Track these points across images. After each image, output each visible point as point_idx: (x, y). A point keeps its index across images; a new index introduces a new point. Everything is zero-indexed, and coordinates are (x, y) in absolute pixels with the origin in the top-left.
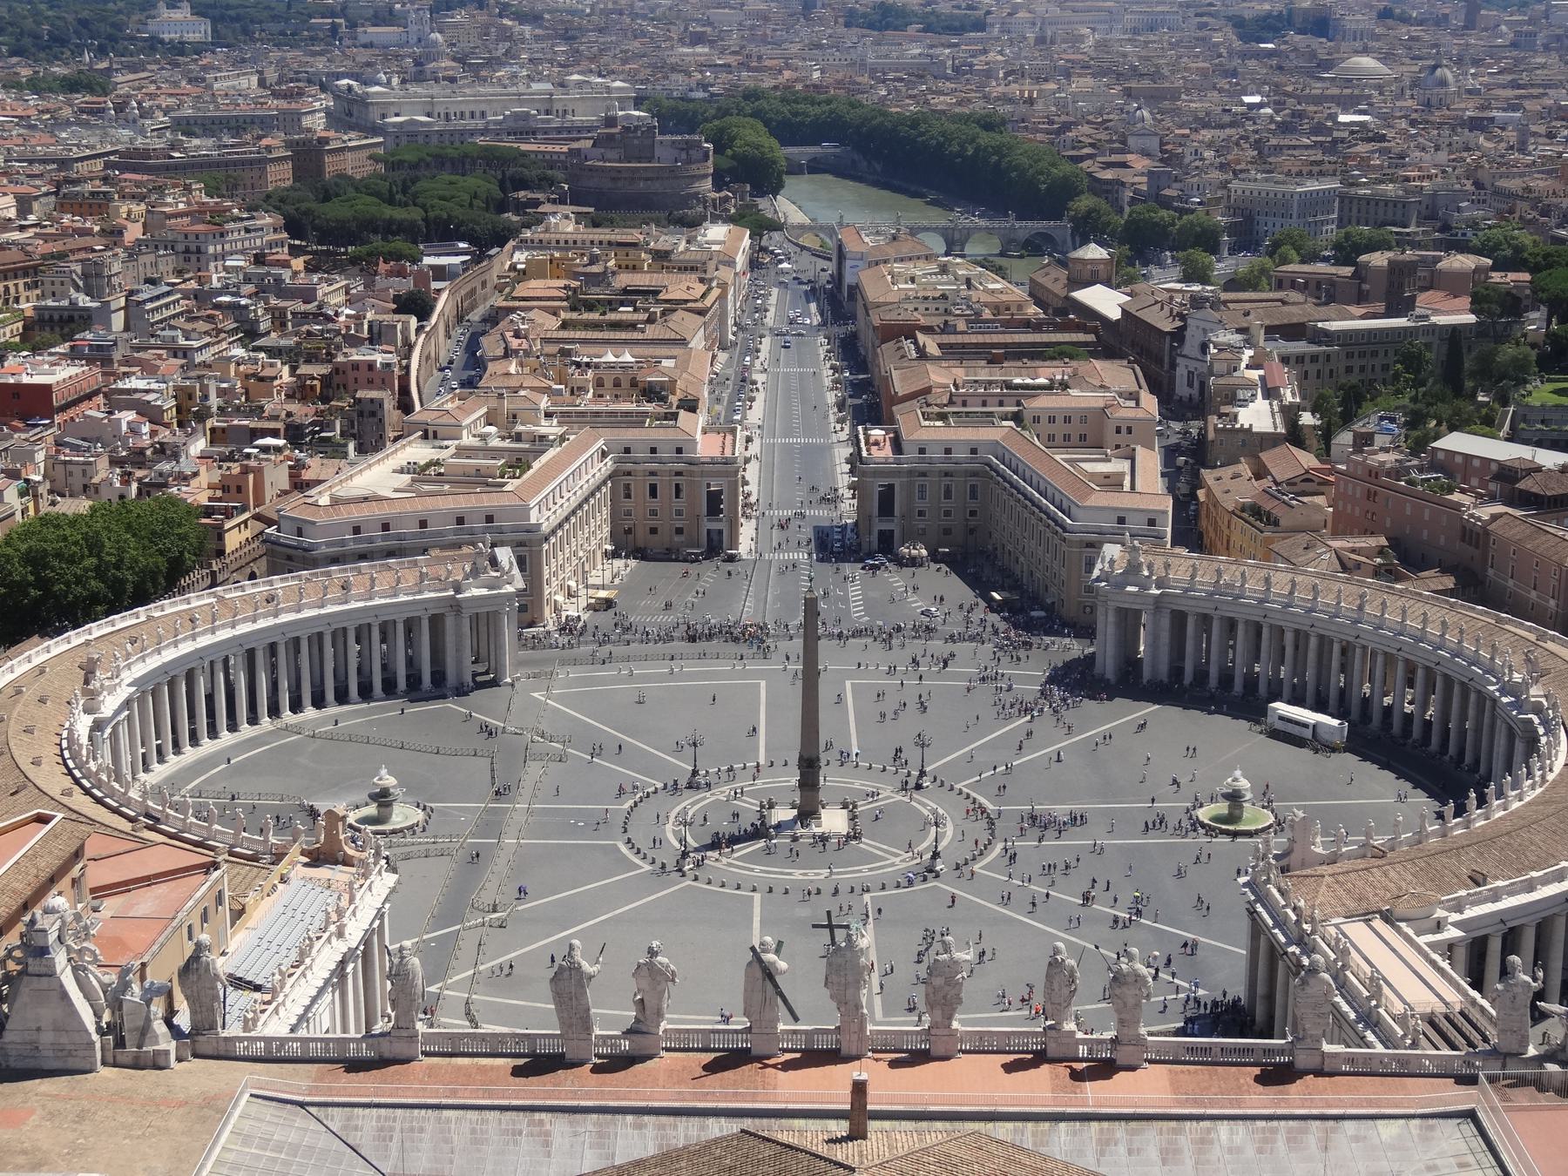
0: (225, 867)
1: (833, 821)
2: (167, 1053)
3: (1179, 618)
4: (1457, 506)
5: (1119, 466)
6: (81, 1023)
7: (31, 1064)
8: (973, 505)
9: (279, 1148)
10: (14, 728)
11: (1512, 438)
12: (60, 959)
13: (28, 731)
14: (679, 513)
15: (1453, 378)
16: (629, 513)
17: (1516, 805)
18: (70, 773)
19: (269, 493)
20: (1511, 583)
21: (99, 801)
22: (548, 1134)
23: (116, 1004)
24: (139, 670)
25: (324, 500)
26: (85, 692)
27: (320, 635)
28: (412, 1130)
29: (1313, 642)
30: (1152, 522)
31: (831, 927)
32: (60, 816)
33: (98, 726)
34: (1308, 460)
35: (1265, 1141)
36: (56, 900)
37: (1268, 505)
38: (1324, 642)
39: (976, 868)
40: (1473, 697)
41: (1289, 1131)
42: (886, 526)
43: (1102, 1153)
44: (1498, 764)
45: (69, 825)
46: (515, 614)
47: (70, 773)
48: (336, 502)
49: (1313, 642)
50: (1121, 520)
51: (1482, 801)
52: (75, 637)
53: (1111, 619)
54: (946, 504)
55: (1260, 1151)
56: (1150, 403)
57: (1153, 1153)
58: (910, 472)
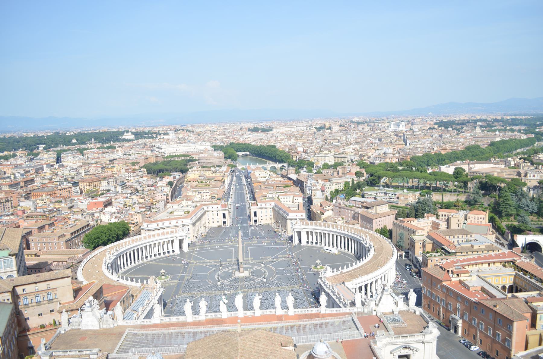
3: (307, 233)
9: (133, 342)
11: (363, 196)
29: (331, 235)
34: (329, 203)
42: (255, 218)
44: (364, 254)
46: (187, 238)
49: (331, 235)
53: (296, 234)
57: (296, 331)
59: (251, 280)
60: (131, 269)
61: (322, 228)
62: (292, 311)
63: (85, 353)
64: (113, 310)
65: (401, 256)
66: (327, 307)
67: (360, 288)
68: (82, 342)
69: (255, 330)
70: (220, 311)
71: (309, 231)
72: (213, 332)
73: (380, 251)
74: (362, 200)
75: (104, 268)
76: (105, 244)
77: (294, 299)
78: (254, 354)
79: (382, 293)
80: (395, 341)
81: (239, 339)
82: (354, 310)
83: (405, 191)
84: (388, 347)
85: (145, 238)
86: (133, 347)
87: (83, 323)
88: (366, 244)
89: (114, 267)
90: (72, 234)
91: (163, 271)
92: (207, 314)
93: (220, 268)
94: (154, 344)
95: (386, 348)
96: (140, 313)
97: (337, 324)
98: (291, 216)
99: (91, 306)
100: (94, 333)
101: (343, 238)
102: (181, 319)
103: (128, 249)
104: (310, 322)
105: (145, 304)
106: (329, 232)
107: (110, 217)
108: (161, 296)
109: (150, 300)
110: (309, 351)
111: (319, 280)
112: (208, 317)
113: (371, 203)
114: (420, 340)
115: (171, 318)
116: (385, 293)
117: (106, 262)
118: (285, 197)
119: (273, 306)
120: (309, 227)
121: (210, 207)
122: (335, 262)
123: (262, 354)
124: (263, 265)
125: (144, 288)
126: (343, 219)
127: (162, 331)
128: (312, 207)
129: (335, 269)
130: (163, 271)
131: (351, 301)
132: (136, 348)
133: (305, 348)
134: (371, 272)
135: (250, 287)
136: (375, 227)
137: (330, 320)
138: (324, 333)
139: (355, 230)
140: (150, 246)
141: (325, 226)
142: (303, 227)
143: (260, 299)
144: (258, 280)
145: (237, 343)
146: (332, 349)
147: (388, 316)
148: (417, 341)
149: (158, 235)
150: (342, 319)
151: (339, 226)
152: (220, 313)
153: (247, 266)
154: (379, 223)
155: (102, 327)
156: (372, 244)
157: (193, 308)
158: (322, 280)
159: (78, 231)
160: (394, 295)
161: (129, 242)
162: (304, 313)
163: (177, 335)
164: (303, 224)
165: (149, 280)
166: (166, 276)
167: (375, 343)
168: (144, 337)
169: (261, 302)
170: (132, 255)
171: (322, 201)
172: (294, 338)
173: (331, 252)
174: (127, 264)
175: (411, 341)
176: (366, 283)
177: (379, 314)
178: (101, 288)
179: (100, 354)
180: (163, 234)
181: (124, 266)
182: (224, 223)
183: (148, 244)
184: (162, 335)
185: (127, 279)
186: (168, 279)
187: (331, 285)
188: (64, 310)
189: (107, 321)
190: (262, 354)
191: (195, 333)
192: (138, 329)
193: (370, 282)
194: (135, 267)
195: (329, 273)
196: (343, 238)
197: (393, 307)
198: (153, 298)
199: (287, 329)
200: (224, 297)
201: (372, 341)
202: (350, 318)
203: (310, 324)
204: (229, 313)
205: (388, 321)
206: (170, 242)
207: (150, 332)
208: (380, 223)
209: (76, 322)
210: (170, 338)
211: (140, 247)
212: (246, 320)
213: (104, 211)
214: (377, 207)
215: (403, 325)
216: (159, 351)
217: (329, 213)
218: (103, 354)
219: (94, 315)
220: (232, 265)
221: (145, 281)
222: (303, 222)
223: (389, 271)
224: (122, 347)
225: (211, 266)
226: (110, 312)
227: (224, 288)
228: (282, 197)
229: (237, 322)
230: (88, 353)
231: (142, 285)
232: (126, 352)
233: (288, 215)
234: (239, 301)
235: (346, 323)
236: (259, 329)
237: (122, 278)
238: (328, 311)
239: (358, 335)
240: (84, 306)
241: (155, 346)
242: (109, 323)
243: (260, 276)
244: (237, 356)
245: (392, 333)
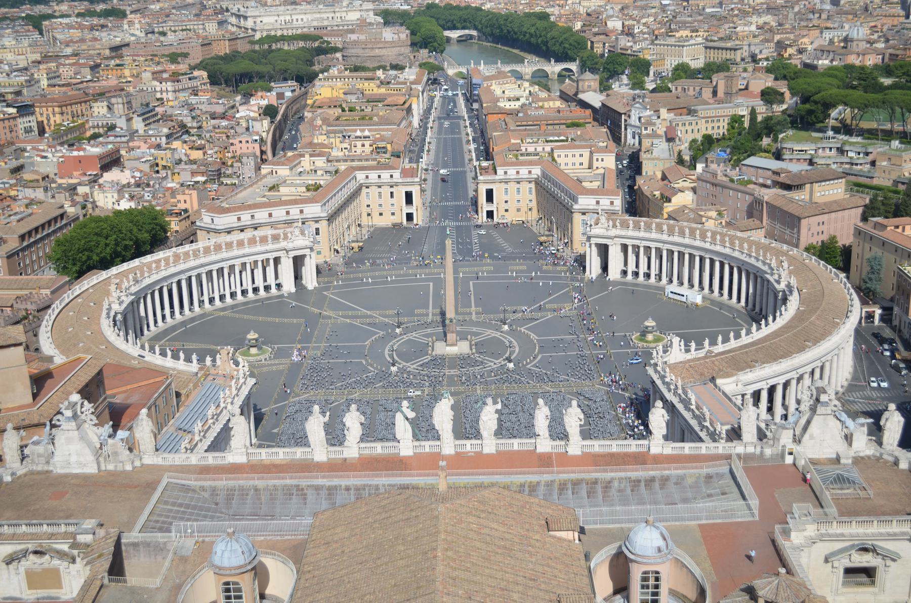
3: (625, 248)
7: (67, 471)
9: (181, 505)
11: (778, 156)
14: (393, 205)
16: (368, 206)
22: (306, 494)
27: (222, 268)
28: (243, 495)
30: (612, 203)
34: (684, 170)
35: (634, 486)
38: (690, 254)
39: (528, 366)
40: (759, 280)
41: (646, 481)
43: (560, 494)
44: (770, 309)
46: (314, 254)
50: (598, 203)
53: (593, 247)
54: (518, 197)
55: (632, 491)
56: (612, 145)
57: (584, 493)
59: (476, 363)
60: (173, 328)
61: (665, 237)
62: (576, 446)
63: (63, 529)
64: (130, 429)
65: (870, 316)
66: (666, 438)
67: (757, 395)
68: (55, 503)
69: (481, 486)
70: (395, 439)
71: (629, 242)
72: (377, 488)
73: (811, 304)
74: (774, 165)
75: (106, 325)
76: (105, 264)
77: (582, 416)
78: (478, 544)
79: (813, 410)
80: (839, 531)
81: (441, 508)
82: (738, 448)
83: (896, 144)
84: (820, 545)
85: (207, 250)
86: (182, 519)
87: (57, 458)
88: (778, 282)
89: (131, 322)
90: (22, 237)
91: (252, 335)
92: (363, 445)
93: (398, 331)
94: (231, 512)
95: (815, 548)
96: (197, 438)
97: (690, 481)
98: (585, 202)
99: (75, 416)
100: (85, 480)
101: (717, 265)
102: (299, 453)
103: (165, 279)
104: (622, 474)
105: (210, 413)
106: (682, 249)
107: (116, 195)
108: (248, 397)
109: (222, 405)
110: (617, 545)
111: (650, 371)
112: (367, 452)
113: (798, 175)
114: (904, 534)
115: (274, 450)
116: (820, 410)
117: (109, 309)
118: (570, 152)
119: (529, 431)
120: (630, 233)
121: (373, 176)
122: (693, 325)
123: (499, 547)
124: (506, 327)
125: (206, 376)
126: (720, 214)
127: (251, 482)
128: (640, 181)
129: (693, 345)
130: (252, 335)
131: (728, 427)
132: (188, 520)
133: (606, 537)
134: (786, 354)
135: (471, 380)
136: (805, 241)
137: (673, 472)
138: (656, 503)
139: (753, 244)
140: (220, 271)
141: (671, 232)
142: (613, 232)
143: (497, 411)
144: (493, 364)
145: (437, 517)
146: (675, 542)
147: (825, 468)
148: (895, 534)
149: (241, 244)
150: (705, 471)
151: (709, 234)
152: (395, 444)
153: (465, 328)
154: (815, 229)
155: (103, 468)
156: (793, 282)
157: (326, 426)
158: (656, 371)
160: (844, 417)
161: (167, 259)
162: (607, 450)
163: (288, 492)
164: (614, 226)
165: (218, 356)
166: (260, 349)
167: (786, 533)
168: (206, 495)
169: (500, 420)
170: (174, 292)
171: (667, 165)
172: (580, 512)
173: (684, 299)
174: (164, 317)
175: (881, 534)
176: (772, 382)
177: (801, 463)
178: (100, 373)
179: (101, 532)
180: (252, 241)
181: (156, 322)
182: (410, 217)
183: (215, 267)
184: (252, 492)
185: (163, 354)
186: (267, 356)
187: (679, 384)
188: (9, 426)
189: (116, 454)
190: (499, 547)
191: (332, 490)
192: (193, 476)
193: (782, 380)
194: (183, 324)
195: (677, 354)
196: (717, 265)
197: (840, 446)
198: (229, 400)
199: (563, 487)
200: (405, 403)
201: (778, 528)
202: (726, 469)
203: (620, 480)
204: (417, 443)
205: (824, 480)
206: (272, 262)
207: (223, 483)
208: (821, 228)
209: (39, 455)
210: (273, 499)
211: (194, 273)
212: (460, 462)
213: (101, 181)
214: (816, 185)
215: (862, 494)
216: (244, 530)
217: (684, 199)
218: (108, 533)
219: (83, 438)
220: (427, 325)
221: (208, 360)
222: (614, 221)
223: (837, 354)
224: (155, 518)
225: (373, 325)
226: (122, 434)
227: (405, 381)
228: (563, 153)
229: (438, 467)
230: (72, 529)
231: (201, 369)
232: (165, 528)
233: (576, 202)
234: (443, 414)
235: (715, 480)
236: (492, 485)
237: (152, 350)
238: (670, 449)
239: (744, 511)
240: (59, 417)
241: (235, 516)
242: (121, 458)
243: (500, 355)
244: (435, 549)
245: (833, 510)
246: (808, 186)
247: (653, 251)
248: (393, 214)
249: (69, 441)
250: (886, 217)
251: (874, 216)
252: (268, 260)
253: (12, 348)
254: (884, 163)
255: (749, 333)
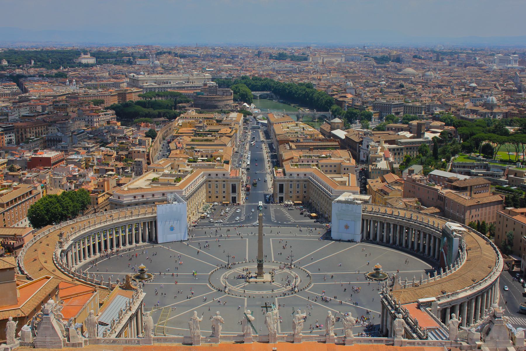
0: (98, 291)
1: (267, 277)
2: (81, 343)
4: (437, 190)
5: (345, 178)
6: (57, 335)
8: (305, 190)
10: (40, 252)
11: (451, 171)
12: (52, 317)
13: (44, 254)
14: (224, 192)
15: (434, 154)
16: (209, 192)
17: (453, 272)
18: (55, 264)
19: (111, 187)
20: (451, 211)
21: (62, 272)
23: (67, 330)
24: (74, 237)
25: (126, 189)
26: (60, 243)
29: (398, 227)
31: (266, 307)
32: (52, 277)
33: (62, 251)
34: (396, 177)
36: (51, 301)
37: (386, 190)
38: (401, 227)
39: (306, 290)
42: (281, 196)
45: (55, 280)
47: (55, 264)
48: (129, 189)
49: (398, 227)
51: (444, 271)
52: (58, 227)
54: (298, 190)
56: (353, 162)
58: (288, 181)
90: (7, 204)
159: (16, 199)
182: (234, 200)
188: (11, 318)
189: (73, 337)
246: (469, 188)
247: (379, 223)
248: (224, 197)
249: (46, 329)
250: (516, 208)
251: (508, 207)
252: (151, 222)
253: (8, 270)
254: (512, 176)
255: (439, 273)
